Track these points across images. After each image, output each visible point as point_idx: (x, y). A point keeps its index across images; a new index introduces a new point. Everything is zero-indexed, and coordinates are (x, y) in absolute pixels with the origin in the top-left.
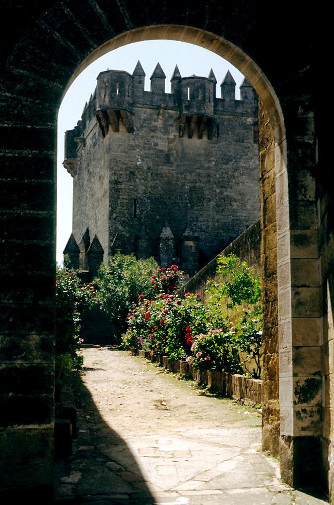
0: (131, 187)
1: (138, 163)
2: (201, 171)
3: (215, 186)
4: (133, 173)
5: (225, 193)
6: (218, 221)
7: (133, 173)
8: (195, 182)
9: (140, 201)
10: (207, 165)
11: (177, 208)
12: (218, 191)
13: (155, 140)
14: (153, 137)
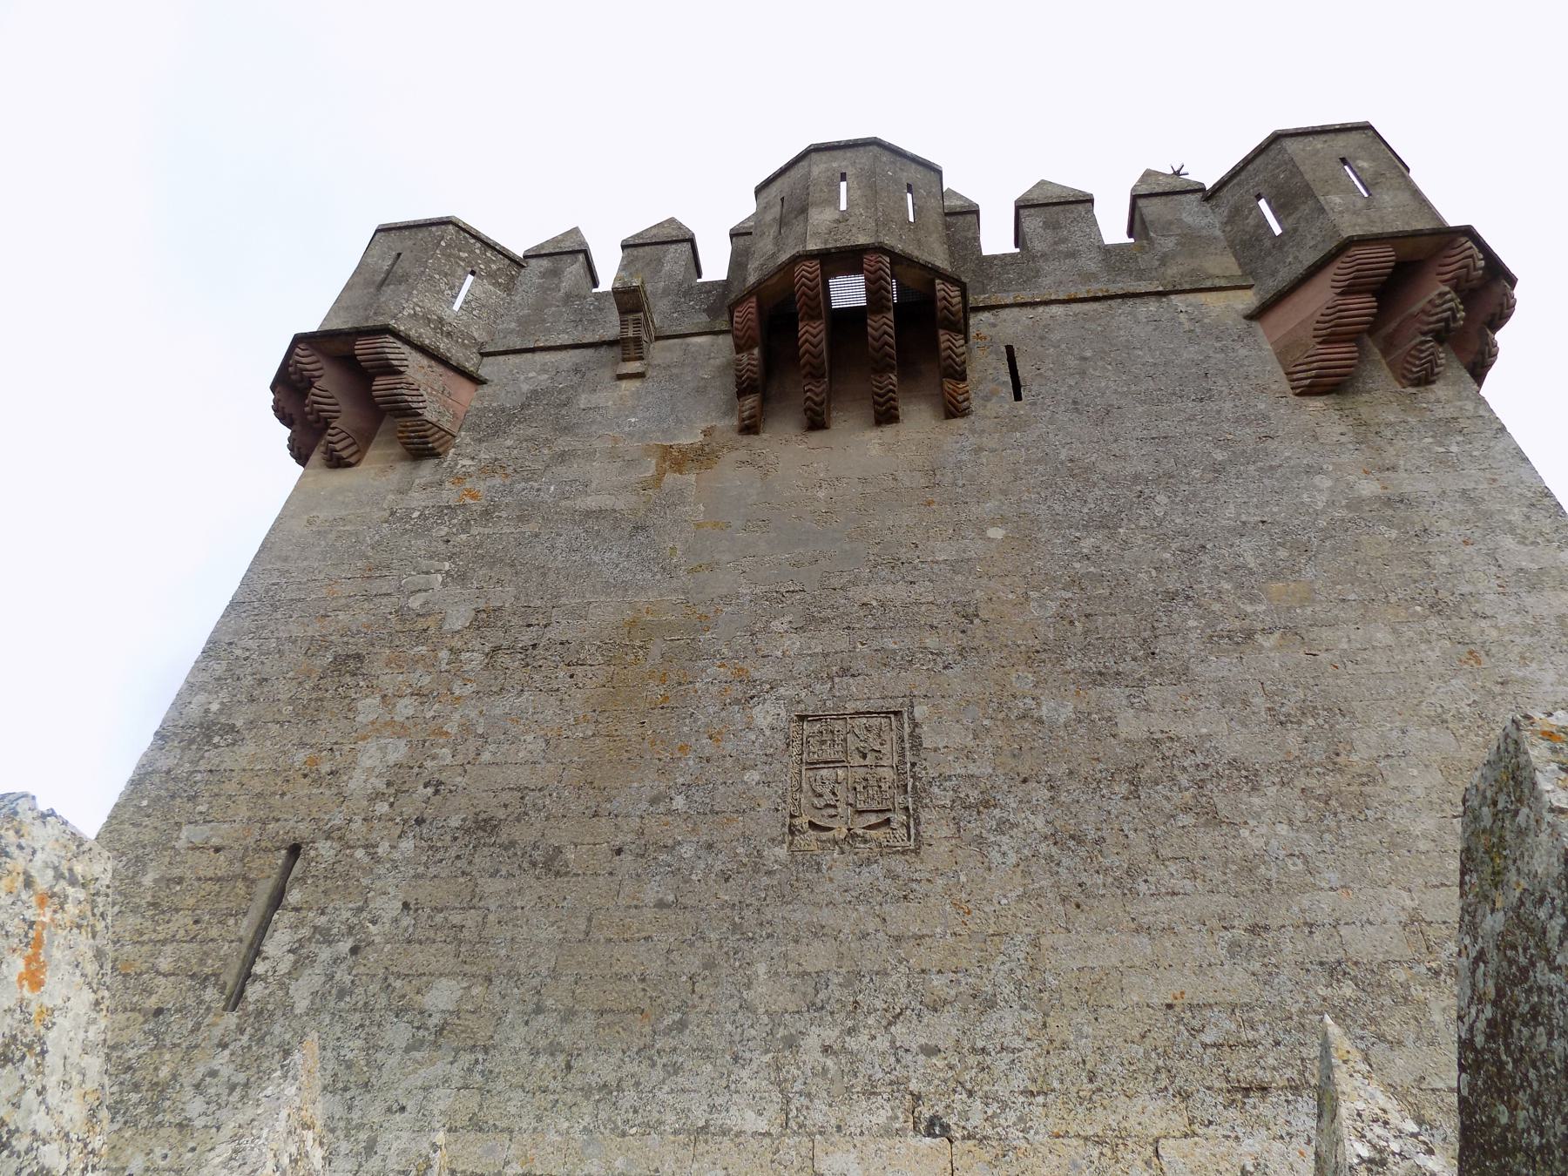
0: (301, 756)
2: (897, 592)
4: (350, 664)
5: (1131, 726)
7: (350, 664)
8: (845, 671)
10: (944, 551)
11: (651, 893)
12: (1058, 709)
13: (573, 470)
14: (562, 457)
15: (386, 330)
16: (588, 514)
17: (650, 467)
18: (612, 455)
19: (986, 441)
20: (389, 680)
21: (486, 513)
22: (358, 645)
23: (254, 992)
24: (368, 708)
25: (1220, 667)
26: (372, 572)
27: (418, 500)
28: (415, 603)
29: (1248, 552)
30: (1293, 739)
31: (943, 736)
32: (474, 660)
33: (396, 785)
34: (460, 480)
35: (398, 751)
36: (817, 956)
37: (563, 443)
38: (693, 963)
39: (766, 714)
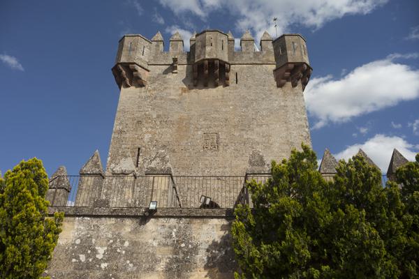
0: (136, 136)
1: (147, 113)
2: (217, 116)
3: (233, 130)
4: (139, 122)
6: (237, 167)
7: (139, 122)
9: (144, 149)
11: (187, 154)
12: (237, 134)
13: (167, 91)
14: (166, 88)
15: (134, 63)
16: (172, 99)
17: (180, 92)
18: (174, 89)
19: (232, 91)
20: (146, 125)
21: (155, 98)
22: (140, 120)
23: (139, 165)
24: (144, 130)
25: (257, 129)
26: (139, 107)
27: (143, 94)
28: (147, 113)
29: (264, 113)
30: (264, 139)
31: (222, 137)
32: (158, 123)
33: (151, 140)
34: (150, 91)
35: (150, 136)
36: (207, 162)
37: (165, 86)
38: (192, 163)
39: (199, 133)
